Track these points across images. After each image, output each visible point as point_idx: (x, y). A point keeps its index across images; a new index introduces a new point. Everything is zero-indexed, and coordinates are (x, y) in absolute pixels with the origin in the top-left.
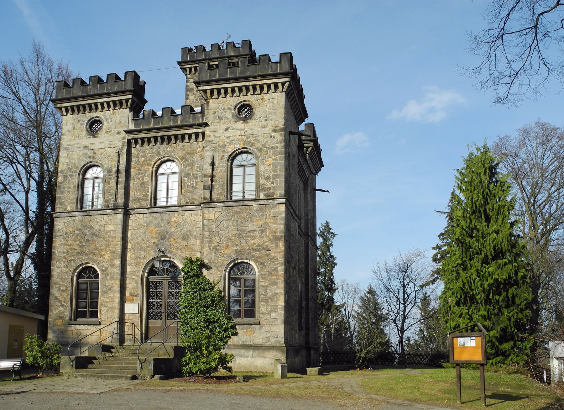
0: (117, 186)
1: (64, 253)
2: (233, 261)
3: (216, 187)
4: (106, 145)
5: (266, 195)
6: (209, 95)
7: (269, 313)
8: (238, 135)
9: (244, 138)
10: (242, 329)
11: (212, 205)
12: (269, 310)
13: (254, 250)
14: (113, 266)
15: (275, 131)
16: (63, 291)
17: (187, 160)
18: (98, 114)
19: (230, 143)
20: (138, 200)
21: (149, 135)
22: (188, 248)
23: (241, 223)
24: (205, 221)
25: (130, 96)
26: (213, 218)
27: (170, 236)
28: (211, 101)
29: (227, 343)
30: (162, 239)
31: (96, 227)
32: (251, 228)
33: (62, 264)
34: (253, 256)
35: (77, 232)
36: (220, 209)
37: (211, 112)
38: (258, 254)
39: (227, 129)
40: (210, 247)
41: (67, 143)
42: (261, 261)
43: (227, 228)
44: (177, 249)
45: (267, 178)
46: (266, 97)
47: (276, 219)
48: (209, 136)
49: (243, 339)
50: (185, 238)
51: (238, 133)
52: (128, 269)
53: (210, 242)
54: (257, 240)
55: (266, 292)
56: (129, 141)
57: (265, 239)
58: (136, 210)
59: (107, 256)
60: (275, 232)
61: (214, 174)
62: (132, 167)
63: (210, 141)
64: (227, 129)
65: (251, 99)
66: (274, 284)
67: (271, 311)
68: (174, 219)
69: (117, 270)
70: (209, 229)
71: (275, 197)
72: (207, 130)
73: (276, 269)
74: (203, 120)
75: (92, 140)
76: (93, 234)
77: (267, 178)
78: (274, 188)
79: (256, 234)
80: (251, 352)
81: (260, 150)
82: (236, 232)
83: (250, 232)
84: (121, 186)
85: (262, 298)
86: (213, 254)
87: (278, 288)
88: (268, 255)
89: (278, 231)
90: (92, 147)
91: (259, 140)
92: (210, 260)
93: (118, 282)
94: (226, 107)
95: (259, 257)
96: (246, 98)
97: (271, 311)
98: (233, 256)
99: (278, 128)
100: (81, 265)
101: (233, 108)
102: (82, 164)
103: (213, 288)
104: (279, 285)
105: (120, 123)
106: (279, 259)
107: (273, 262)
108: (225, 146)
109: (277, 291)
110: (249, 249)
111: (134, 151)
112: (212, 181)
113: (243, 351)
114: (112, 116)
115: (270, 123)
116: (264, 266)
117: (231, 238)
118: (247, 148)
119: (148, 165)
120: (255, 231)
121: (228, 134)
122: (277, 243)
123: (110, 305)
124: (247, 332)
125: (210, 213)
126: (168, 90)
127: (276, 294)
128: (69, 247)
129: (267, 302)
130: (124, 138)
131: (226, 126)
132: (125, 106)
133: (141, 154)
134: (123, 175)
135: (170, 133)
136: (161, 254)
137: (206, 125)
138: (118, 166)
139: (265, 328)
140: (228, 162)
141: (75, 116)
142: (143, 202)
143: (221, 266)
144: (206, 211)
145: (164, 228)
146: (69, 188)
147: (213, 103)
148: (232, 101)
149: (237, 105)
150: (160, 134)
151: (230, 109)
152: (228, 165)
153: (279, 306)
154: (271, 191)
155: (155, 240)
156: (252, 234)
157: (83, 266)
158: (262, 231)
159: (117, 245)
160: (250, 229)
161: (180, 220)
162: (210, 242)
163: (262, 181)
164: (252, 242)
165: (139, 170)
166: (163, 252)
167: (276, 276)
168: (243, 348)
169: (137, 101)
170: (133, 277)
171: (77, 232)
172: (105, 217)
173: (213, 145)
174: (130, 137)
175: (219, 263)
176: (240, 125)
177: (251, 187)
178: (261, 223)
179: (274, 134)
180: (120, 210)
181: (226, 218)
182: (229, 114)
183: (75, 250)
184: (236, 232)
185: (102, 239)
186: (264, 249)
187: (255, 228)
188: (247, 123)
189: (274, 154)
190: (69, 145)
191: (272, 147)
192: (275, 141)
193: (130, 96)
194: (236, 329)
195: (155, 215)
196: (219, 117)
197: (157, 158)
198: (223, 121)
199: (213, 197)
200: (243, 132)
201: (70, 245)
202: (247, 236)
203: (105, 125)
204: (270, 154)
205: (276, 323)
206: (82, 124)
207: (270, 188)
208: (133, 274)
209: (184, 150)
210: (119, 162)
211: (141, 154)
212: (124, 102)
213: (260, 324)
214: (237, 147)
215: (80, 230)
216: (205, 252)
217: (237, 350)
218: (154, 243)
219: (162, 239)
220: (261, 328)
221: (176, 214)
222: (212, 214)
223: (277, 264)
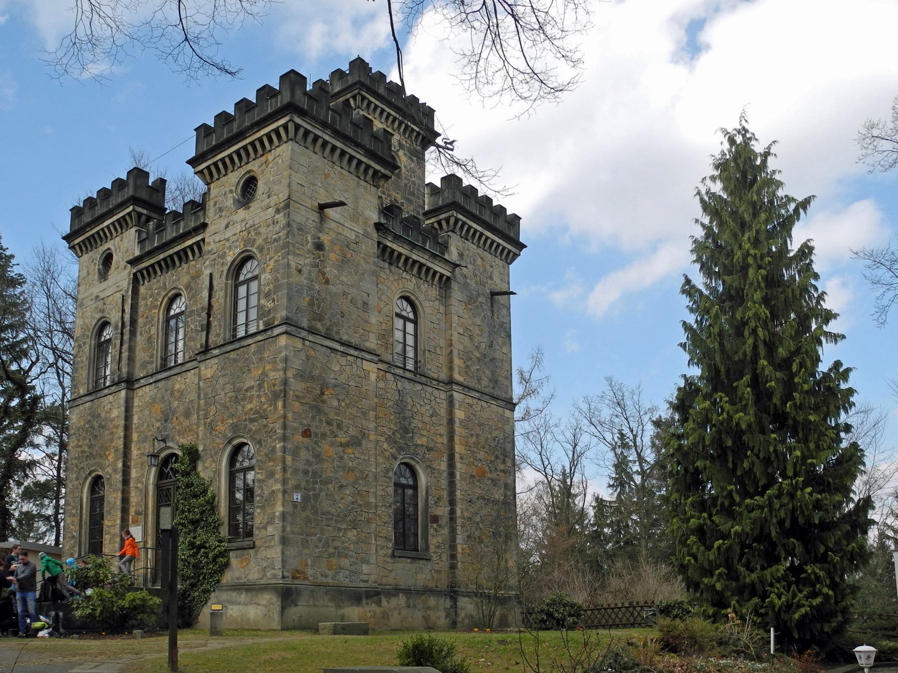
0: (121, 349)
1: (76, 458)
2: (230, 442)
3: (214, 323)
4: (114, 289)
5: (266, 324)
6: (208, 178)
7: (265, 528)
8: (238, 231)
9: (245, 233)
10: (237, 557)
11: (208, 356)
12: (265, 522)
13: (252, 420)
14: (115, 471)
15: (278, 211)
16: (74, 515)
17: (192, 289)
18: (109, 245)
19: (230, 248)
20: (144, 366)
21: (152, 261)
22: (190, 431)
23: (238, 376)
24: (201, 384)
25: (131, 208)
26: (209, 376)
27: (174, 413)
28: (212, 185)
29: (218, 581)
30: (166, 421)
31: (103, 415)
32: (248, 384)
33: (74, 476)
34: (250, 430)
35: (87, 426)
36: (216, 360)
37: (211, 203)
38: (254, 427)
39: (227, 227)
40: (205, 423)
41: (83, 296)
42: (257, 437)
43: (223, 389)
44: (180, 433)
45: (267, 295)
46: (270, 157)
47: (275, 362)
48: (209, 243)
49: (237, 574)
50: (187, 415)
51: (238, 228)
52: (134, 474)
53: (206, 416)
54: (254, 402)
55: (262, 490)
56: (135, 275)
57: (263, 400)
58: (142, 381)
59: (111, 458)
60: (274, 385)
61: (213, 304)
62: (140, 314)
63: (209, 252)
64: (227, 227)
65: (254, 166)
66: (271, 475)
67: (268, 523)
68: (177, 386)
69: (119, 477)
70: (206, 395)
71: (276, 323)
72: (207, 235)
73: (274, 449)
74: (204, 219)
75: (105, 284)
76: (101, 427)
77: (267, 295)
78: (275, 309)
79: (254, 392)
80: (243, 597)
81: (261, 249)
82: (233, 394)
83: (247, 390)
84: (125, 347)
85: (258, 502)
86: (208, 435)
87: (276, 481)
88: (265, 426)
89: (277, 382)
90: (102, 296)
91: (260, 233)
92: (205, 446)
93: (120, 495)
94: (227, 189)
95: (256, 431)
96: (249, 167)
97: (268, 523)
98: (229, 435)
99: (282, 205)
100: (90, 474)
101: (234, 188)
102: (94, 323)
103: (205, 492)
104: (277, 476)
105: (127, 251)
106: (278, 431)
107: (271, 437)
108: (223, 256)
109: (275, 488)
110: (245, 420)
111: (142, 290)
112: (209, 315)
113: (234, 594)
114: (121, 243)
115: (274, 200)
116: (261, 446)
117: (228, 404)
118: (248, 251)
119: (155, 307)
120: (252, 387)
121: (228, 234)
122: (276, 404)
123: (112, 531)
124: (241, 562)
125: (206, 368)
126: (181, 183)
127: (273, 492)
128: (80, 450)
129: (263, 508)
130: (129, 274)
131: (225, 223)
132: (130, 225)
133: (149, 292)
134: (128, 328)
135: (171, 252)
136: (163, 445)
137: (204, 226)
138: (123, 317)
139: (262, 553)
140: (227, 279)
141: (91, 253)
142: (149, 366)
143: (216, 453)
144: (202, 366)
145: (167, 403)
146: (82, 362)
147: (216, 190)
148: (234, 178)
149: (239, 182)
150: (162, 256)
151: (231, 191)
152: (226, 284)
153: (277, 514)
154: (272, 315)
155: (158, 424)
156: (249, 394)
157: (93, 475)
158: (260, 386)
159: (120, 438)
160: (248, 386)
161: (183, 387)
162: (206, 416)
163: (263, 301)
164: (249, 406)
165: (147, 317)
166: (164, 441)
167: (274, 460)
168: (234, 590)
169: (145, 212)
170: (139, 485)
171: (87, 426)
172: (111, 398)
173: (213, 257)
174: (134, 271)
175: (214, 448)
176: (242, 213)
177: (253, 314)
178: (260, 372)
179: (277, 216)
180: (123, 384)
181: (223, 372)
182: (229, 202)
183: (85, 452)
184: (233, 394)
185: (107, 432)
186: (261, 417)
187: (253, 383)
188: (249, 208)
189: (276, 252)
190: (83, 299)
191: (275, 240)
192: (277, 228)
193: (131, 208)
194: (228, 557)
195: (160, 384)
196: (221, 210)
197: (163, 294)
198: (223, 214)
199: (210, 341)
200: (243, 224)
201: (81, 446)
202: (244, 399)
203: (115, 257)
204: (272, 254)
205: (273, 544)
206: (95, 264)
207: (269, 312)
208: (138, 480)
209: (188, 273)
210: (123, 311)
211: (149, 292)
212: (127, 218)
213: (253, 548)
214: (238, 251)
215: (89, 422)
216: (200, 433)
217: (229, 593)
218: (158, 428)
219: (166, 421)
220: (256, 553)
221: (179, 378)
222: (209, 369)
223: (275, 440)
